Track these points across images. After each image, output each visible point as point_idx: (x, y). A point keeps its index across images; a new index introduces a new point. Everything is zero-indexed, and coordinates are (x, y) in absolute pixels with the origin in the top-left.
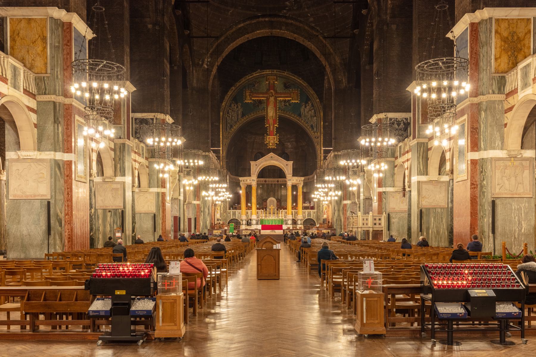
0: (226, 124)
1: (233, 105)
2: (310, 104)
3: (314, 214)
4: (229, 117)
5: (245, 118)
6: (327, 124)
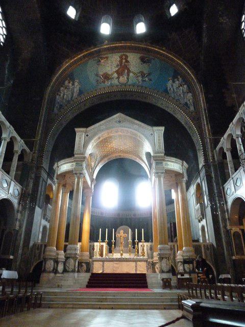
1: (67, 82)
2: (180, 79)
3: (208, 252)
4: (60, 95)
5: (83, 96)
6: (211, 96)
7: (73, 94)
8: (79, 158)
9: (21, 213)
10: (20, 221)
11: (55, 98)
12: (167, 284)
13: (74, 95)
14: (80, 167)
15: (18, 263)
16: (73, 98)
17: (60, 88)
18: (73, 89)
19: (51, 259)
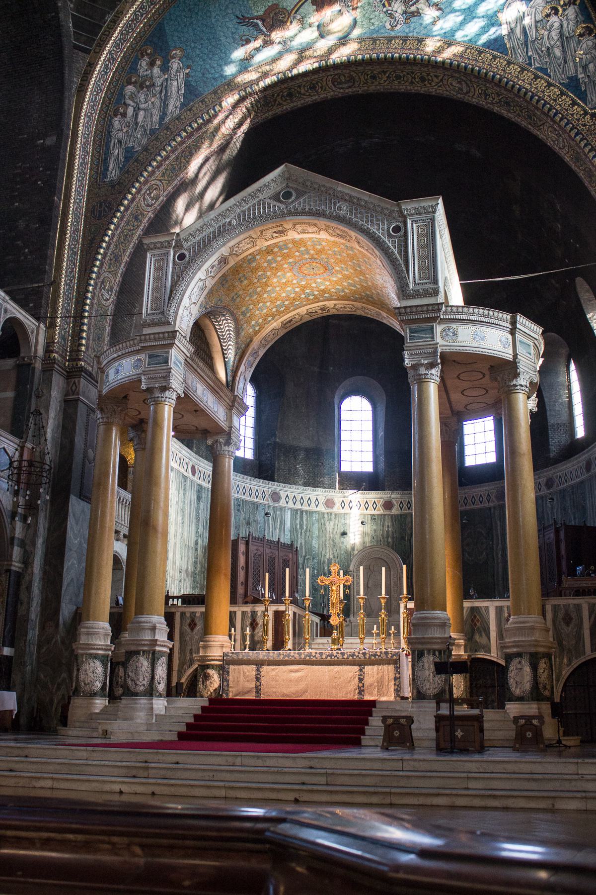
0: (108, 148)
1: (144, 63)
4: (124, 115)
7: (165, 105)
8: (157, 336)
9: (24, 519)
10: (22, 544)
11: (111, 125)
12: (397, 733)
13: (171, 108)
14: (158, 367)
15: (29, 668)
16: (167, 120)
17: (123, 88)
18: (165, 88)
19: (96, 657)
